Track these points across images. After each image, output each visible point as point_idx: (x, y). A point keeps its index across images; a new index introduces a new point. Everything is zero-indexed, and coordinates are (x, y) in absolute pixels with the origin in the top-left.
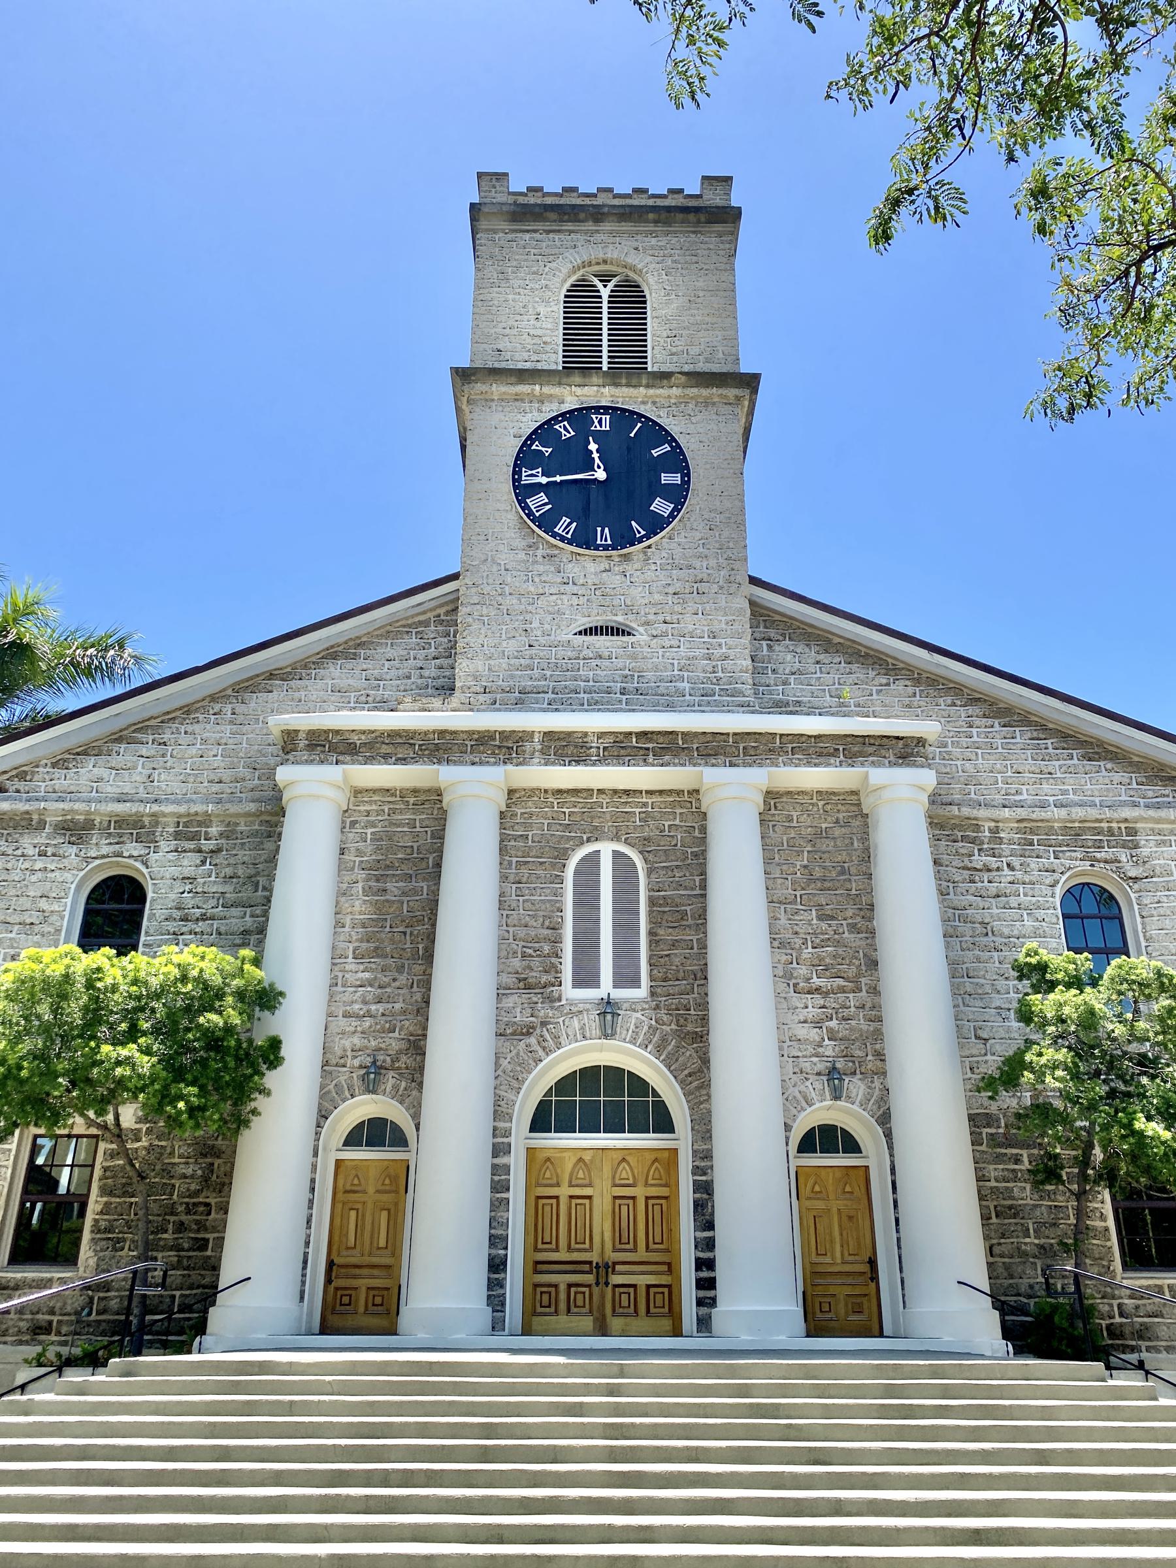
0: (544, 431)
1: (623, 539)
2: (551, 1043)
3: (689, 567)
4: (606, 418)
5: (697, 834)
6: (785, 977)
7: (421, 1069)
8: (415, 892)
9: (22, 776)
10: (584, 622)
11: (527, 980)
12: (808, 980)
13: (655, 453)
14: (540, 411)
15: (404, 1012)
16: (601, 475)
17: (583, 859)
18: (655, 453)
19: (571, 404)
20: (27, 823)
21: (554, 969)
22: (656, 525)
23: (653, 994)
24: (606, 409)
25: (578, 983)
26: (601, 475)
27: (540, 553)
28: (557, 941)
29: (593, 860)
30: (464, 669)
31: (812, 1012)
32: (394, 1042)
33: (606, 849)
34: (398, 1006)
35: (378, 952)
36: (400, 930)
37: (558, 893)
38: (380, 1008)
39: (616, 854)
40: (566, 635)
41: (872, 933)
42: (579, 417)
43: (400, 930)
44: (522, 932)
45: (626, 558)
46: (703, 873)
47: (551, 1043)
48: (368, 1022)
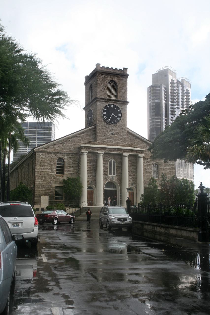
0: (106, 107)
1: (115, 123)
2: (107, 180)
3: (121, 127)
4: (113, 106)
5: (121, 159)
6: (129, 174)
7: (96, 182)
8: (94, 164)
9: (49, 147)
10: (110, 133)
11: (105, 174)
12: (130, 175)
13: (118, 111)
14: (105, 104)
15: (93, 177)
16: (112, 114)
17: (110, 161)
18: (118, 111)
19: (109, 103)
20: (51, 153)
21: (108, 173)
22: (118, 121)
23: (117, 176)
24: (113, 105)
25: (110, 174)
26: (112, 114)
27: (105, 124)
28: (108, 170)
29: (111, 162)
30: (98, 138)
31: (130, 178)
32: (93, 179)
33: (112, 160)
34: (93, 176)
35: (91, 170)
36: (93, 169)
37: (108, 165)
38: (91, 176)
39: (113, 161)
40: (108, 135)
41: (136, 170)
42: (110, 105)
43: (93, 169)
44: (104, 169)
45: (114, 125)
46: (122, 163)
47: (107, 180)
48: (90, 177)
